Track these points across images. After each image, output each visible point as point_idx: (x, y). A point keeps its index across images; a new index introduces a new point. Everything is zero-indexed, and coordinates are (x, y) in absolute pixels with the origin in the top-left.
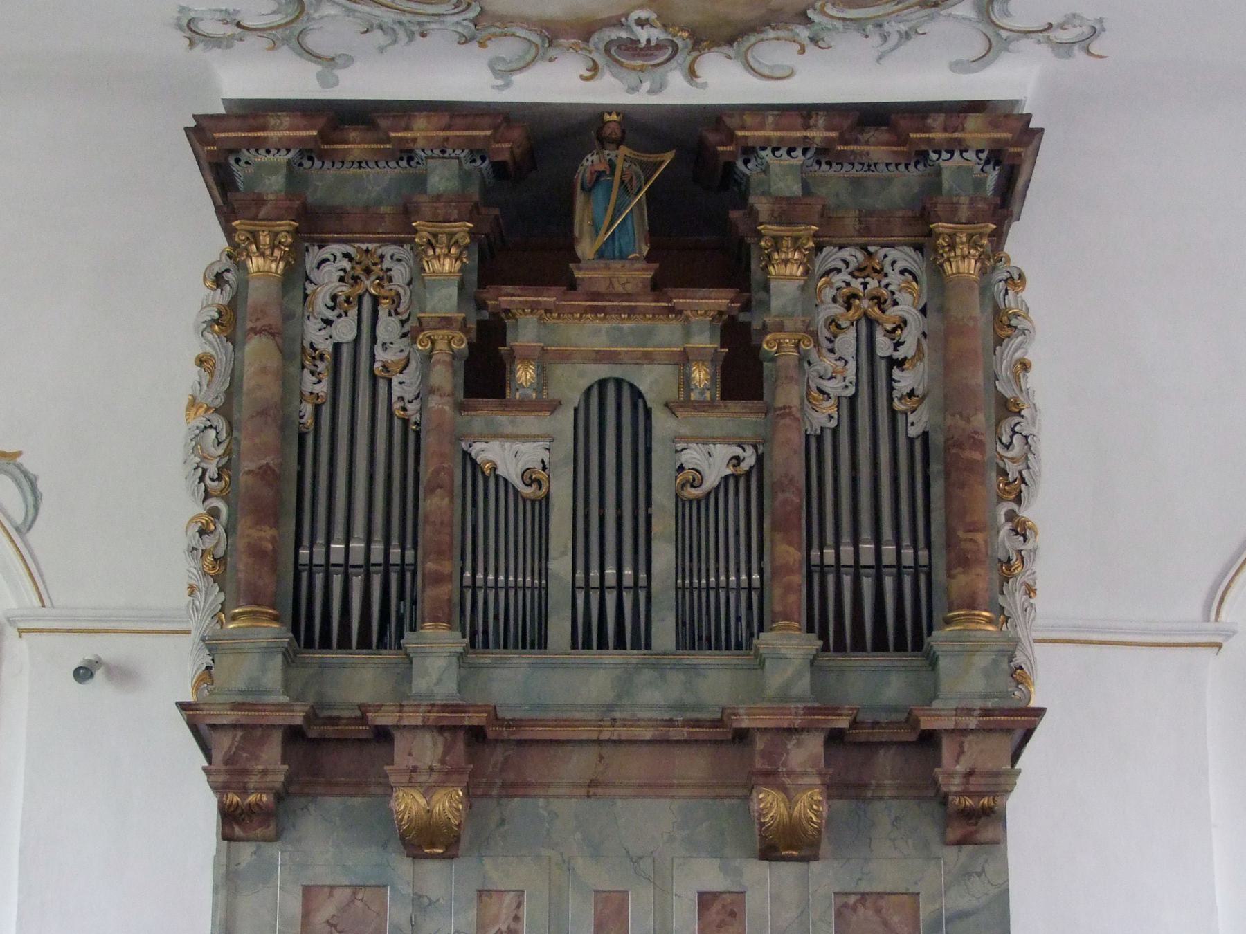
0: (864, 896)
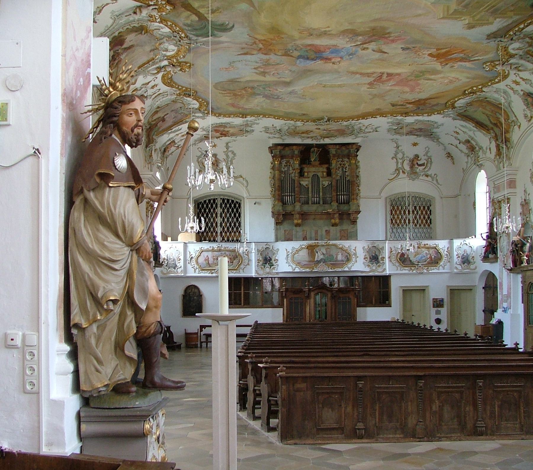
0: (342, 230)
